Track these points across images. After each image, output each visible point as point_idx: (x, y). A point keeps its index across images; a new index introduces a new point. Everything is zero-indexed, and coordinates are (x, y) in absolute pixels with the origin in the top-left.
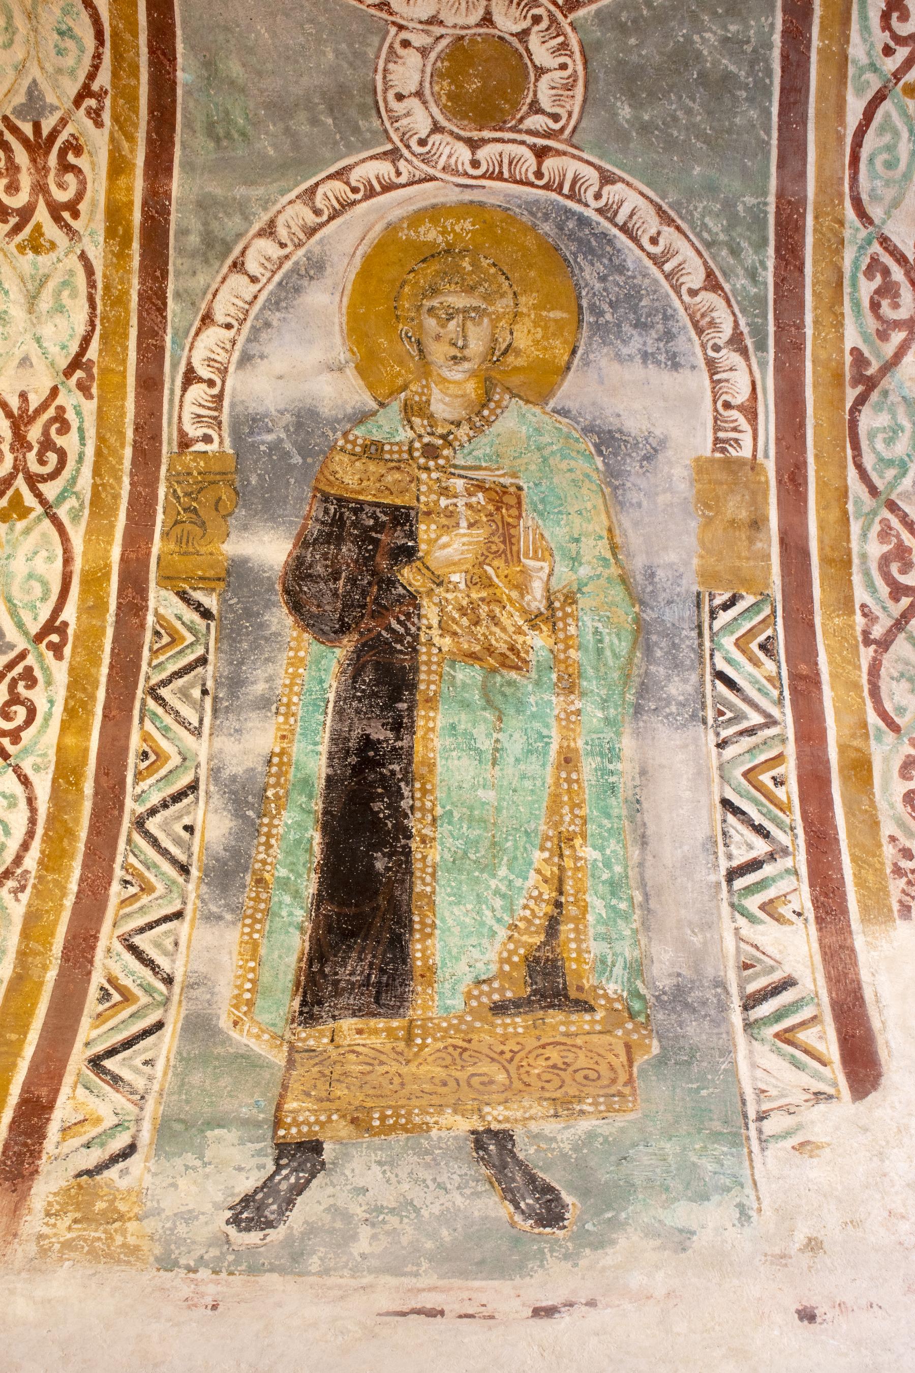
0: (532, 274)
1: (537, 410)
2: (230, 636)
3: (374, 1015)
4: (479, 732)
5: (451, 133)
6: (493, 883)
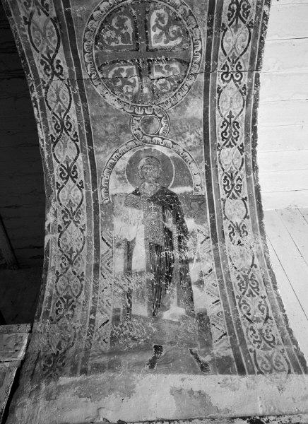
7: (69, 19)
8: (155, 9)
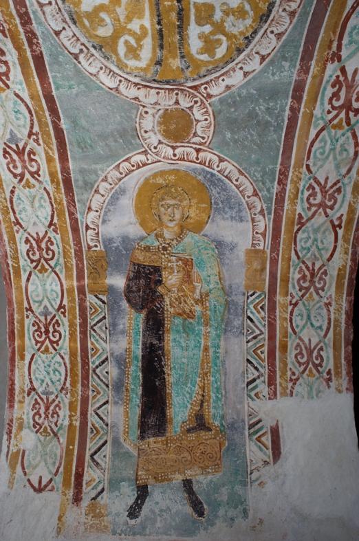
0: (195, 192)
1: (197, 235)
2: (111, 310)
3: (158, 436)
4: (182, 341)
5: (166, 144)
6: (187, 389)
7: (307, 56)
8: (145, 70)
